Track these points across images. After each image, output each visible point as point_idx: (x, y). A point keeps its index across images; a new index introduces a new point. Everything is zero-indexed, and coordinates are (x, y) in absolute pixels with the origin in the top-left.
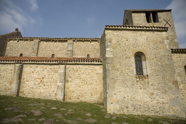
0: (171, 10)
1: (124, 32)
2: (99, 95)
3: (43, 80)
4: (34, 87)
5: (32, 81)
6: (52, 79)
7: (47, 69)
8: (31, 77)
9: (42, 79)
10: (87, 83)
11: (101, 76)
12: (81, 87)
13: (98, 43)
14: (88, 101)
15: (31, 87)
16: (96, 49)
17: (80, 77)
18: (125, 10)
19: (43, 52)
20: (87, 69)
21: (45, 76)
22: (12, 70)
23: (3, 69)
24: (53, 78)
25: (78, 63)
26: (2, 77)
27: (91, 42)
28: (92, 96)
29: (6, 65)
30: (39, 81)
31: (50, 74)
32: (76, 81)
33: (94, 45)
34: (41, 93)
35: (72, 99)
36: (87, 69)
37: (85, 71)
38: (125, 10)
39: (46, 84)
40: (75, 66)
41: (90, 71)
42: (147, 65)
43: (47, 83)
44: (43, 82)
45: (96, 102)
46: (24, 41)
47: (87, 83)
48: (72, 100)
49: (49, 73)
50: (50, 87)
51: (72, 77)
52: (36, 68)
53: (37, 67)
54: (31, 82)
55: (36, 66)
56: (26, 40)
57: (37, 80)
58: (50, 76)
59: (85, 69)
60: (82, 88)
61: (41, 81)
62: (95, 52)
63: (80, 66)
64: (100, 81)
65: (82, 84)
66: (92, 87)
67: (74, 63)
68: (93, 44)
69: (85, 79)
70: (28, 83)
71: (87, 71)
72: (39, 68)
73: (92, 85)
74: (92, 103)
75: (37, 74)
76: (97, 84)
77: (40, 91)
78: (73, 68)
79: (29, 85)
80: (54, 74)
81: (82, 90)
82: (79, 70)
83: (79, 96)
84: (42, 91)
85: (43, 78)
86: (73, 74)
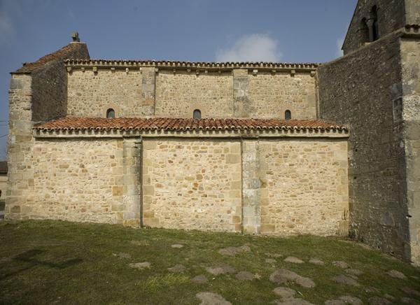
5: (170, 184)
7: (206, 152)
8: (168, 175)
9: (196, 181)
11: (344, 170)
17: (295, 172)
21: (204, 171)
22: (113, 157)
26: (92, 175)
29: (96, 142)
30: (191, 185)
34: (197, 217)
36: (310, 150)
37: (304, 157)
39: (208, 193)
43: (210, 189)
44: (201, 188)
49: (215, 162)
50: (220, 200)
52: (178, 151)
54: (170, 187)
57: (185, 182)
58: (218, 171)
59: (306, 150)
69: (306, 177)
70: (160, 190)
71: (312, 156)
72: (185, 149)
75: (183, 165)
77: (196, 211)
79: (166, 196)
80: (226, 167)
81: (299, 205)
82: (291, 154)
84: (199, 211)
85: (199, 177)
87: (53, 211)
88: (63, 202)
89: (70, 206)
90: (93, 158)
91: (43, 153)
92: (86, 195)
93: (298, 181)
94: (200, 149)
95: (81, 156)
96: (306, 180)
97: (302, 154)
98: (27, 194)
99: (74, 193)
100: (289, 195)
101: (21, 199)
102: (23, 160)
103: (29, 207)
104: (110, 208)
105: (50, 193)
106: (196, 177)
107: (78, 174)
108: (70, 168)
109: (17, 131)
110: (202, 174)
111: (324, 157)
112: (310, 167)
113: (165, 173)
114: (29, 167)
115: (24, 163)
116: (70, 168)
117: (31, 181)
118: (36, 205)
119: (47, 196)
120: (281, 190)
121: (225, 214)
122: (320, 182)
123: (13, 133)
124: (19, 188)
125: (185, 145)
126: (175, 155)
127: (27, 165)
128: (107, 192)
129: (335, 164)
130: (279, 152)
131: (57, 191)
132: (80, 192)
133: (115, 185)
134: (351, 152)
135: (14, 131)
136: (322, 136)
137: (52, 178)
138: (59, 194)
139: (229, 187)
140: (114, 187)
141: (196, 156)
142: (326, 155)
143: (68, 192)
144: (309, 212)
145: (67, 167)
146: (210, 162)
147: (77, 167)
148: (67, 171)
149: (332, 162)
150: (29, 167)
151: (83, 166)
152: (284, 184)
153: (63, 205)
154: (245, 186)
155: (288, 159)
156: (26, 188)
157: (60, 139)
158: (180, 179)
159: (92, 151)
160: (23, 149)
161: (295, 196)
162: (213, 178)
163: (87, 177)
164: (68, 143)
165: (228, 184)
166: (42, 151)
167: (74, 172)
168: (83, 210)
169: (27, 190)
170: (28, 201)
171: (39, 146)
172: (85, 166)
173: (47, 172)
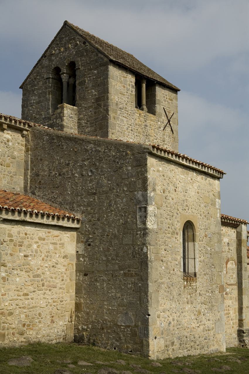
0: (179, 90)
1: (173, 167)
2: (67, 318)
10: (43, 285)
11: (72, 265)
12: (29, 297)
13: (21, 138)
14: (43, 340)
16: (14, 158)
17: (29, 265)
18: (66, 23)
20: (44, 239)
25: (28, 219)
28: (53, 322)
33: (10, 144)
35: (7, 337)
36: (44, 239)
37: (38, 247)
38: (66, 23)
40: (16, 229)
41: (51, 247)
42: (197, 252)
45: (61, 340)
47: (43, 285)
48: (6, 342)
51: (9, 265)
59: (41, 239)
60: (32, 299)
62: (12, 169)
63: (29, 229)
64: (70, 279)
65: (33, 289)
66: (55, 296)
67: (18, 218)
68: (8, 141)
69: (39, 272)
73: (54, 290)
74: (54, 342)
76: (64, 286)
78: (10, 235)
81: (31, 306)
82: (26, 243)
83: (24, 325)
86: (11, 255)
93: (31, 276)
96: (38, 276)
100: (22, 293)
111: (55, 249)
112: (43, 260)
120: (13, 287)
122: (52, 278)
129: (65, 257)
130: (14, 238)
134: (82, 246)
136: (57, 224)
142: (58, 246)
144: (40, 314)
149: (63, 255)
152: (18, 279)
155: (23, 248)
161: (27, 295)
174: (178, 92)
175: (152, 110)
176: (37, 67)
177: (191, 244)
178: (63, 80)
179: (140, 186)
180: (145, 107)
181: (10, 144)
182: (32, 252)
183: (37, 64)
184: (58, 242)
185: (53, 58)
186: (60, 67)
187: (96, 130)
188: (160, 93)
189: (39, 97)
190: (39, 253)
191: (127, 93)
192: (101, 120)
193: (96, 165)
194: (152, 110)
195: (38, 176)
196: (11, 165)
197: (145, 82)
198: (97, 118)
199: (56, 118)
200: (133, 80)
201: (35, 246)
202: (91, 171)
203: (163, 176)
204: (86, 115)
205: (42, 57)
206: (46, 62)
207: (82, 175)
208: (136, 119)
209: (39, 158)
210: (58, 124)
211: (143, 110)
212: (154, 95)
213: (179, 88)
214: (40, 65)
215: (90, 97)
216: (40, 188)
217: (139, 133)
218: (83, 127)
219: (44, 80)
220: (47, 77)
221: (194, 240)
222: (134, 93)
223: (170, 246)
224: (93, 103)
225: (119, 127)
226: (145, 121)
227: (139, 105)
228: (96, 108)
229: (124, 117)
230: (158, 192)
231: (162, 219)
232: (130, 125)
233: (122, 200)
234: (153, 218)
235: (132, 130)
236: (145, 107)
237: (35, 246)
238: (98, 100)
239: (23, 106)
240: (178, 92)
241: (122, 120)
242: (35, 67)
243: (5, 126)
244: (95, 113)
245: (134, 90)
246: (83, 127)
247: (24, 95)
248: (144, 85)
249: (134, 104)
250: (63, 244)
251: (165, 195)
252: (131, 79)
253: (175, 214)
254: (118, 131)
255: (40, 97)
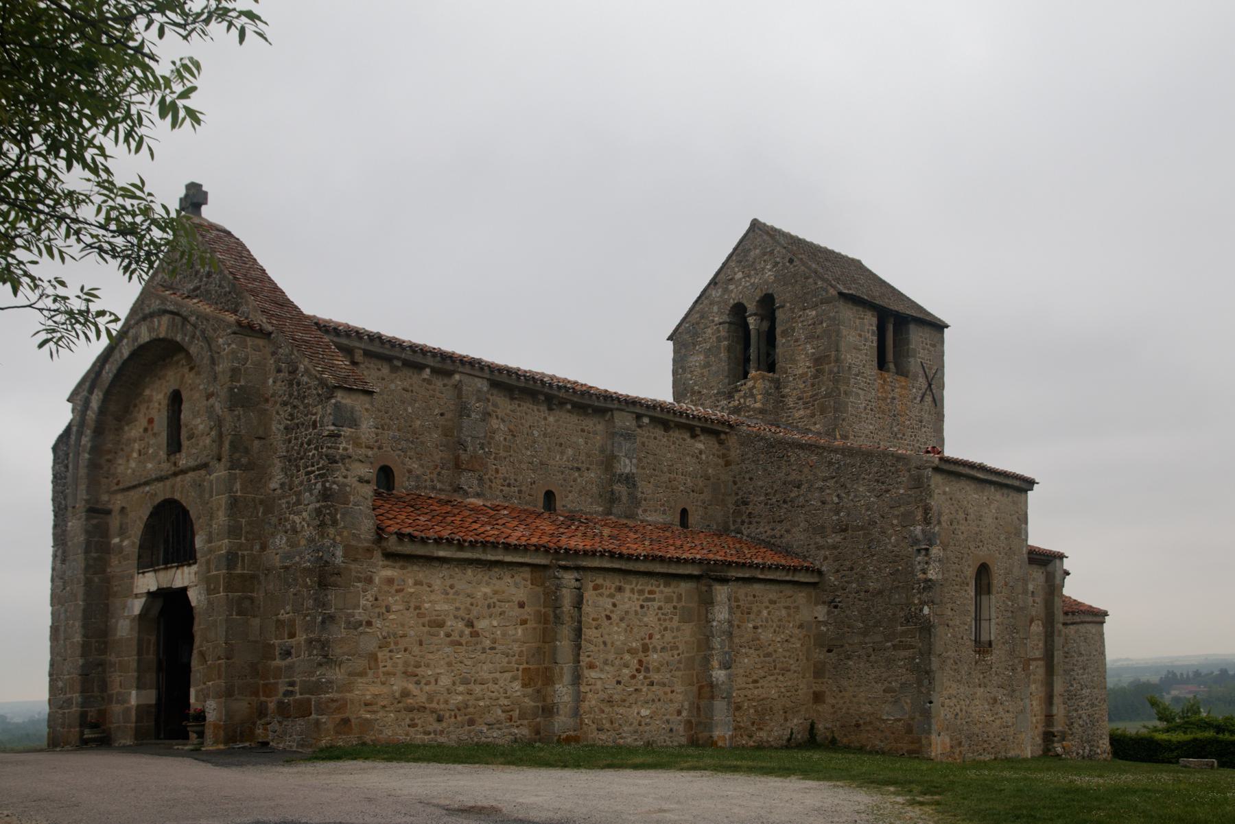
0: (947, 326)
1: (963, 483)
3: (644, 659)
4: (616, 697)
5: (606, 662)
6: (676, 652)
7: (654, 600)
8: (605, 643)
9: (641, 655)
13: (717, 446)
15: (605, 696)
19: (503, 470)
21: (651, 637)
22: (521, 605)
23: (485, 596)
24: (677, 648)
26: (488, 643)
27: (694, 436)
29: (496, 571)
30: (634, 663)
31: (666, 629)
32: (746, 660)
33: (704, 457)
37: (769, 613)
39: (656, 677)
43: (658, 670)
44: (647, 670)
46: (394, 369)
49: (665, 620)
52: (618, 596)
53: (620, 589)
55: (617, 581)
56: (408, 364)
57: (627, 657)
58: (668, 636)
59: (772, 602)
61: (640, 662)
68: (701, 452)
70: (593, 674)
71: (777, 613)
72: (627, 594)
75: (623, 625)
80: (678, 629)
82: (755, 609)
84: (644, 712)
85: (645, 649)
87: (414, 725)
88: (434, 705)
89: (447, 715)
90: (489, 607)
91: (397, 591)
92: (477, 689)
94: (646, 595)
95: (469, 600)
97: (767, 607)
98: (366, 689)
99: (454, 684)
101: (352, 702)
102: (357, 606)
103: (366, 719)
104: (516, 714)
105: (411, 687)
106: (641, 650)
107: (463, 641)
108: (447, 629)
109: (345, 534)
110: (647, 641)
113: (601, 640)
114: (369, 624)
115: (359, 614)
116: (447, 629)
117: (373, 657)
118: (381, 714)
119: (405, 694)
121: (674, 718)
123: (338, 538)
124: (350, 674)
125: (632, 584)
126: (614, 605)
127: (365, 618)
128: (514, 679)
131: (423, 681)
132: (465, 682)
133: (525, 666)
135: (340, 534)
136: (792, 579)
137: (416, 649)
138: (427, 688)
139: (682, 666)
140: (524, 669)
141: (642, 607)
143: (445, 681)
145: (441, 625)
146: (659, 620)
147: (461, 625)
148: (442, 634)
150: (369, 624)
151: (470, 624)
153: (433, 711)
154: (715, 663)
155: (752, 616)
156: (363, 674)
157: (430, 560)
158: (619, 653)
159: (487, 590)
160: (359, 580)
162: (663, 649)
163: (479, 647)
164: (445, 571)
165: (680, 662)
166: (395, 587)
167: (456, 637)
168: (471, 722)
169: (364, 680)
170: (366, 705)
171: (388, 573)
172: (475, 623)
173: (404, 636)
174: (945, 329)
175: (902, 372)
176: (700, 302)
177: (984, 597)
178: (751, 327)
179: (919, 517)
180: (892, 366)
181: (704, 457)
182: (762, 621)
183: (699, 298)
184: (792, 606)
185: (731, 287)
186: (746, 304)
187: (815, 415)
188: (917, 337)
189: (707, 357)
190: (770, 622)
191: (865, 345)
192: (825, 397)
193: (846, 487)
194: (902, 372)
195: (746, 503)
196: (705, 490)
197: (892, 320)
198: (817, 394)
199: (745, 397)
200: (874, 321)
201: (765, 613)
202: (838, 496)
203: (951, 499)
204: (795, 389)
205: (709, 285)
206: (716, 294)
207: (823, 503)
208: (878, 390)
209: (747, 476)
210: (748, 406)
211: (888, 371)
212: (908, 342)
213: (947, 321)
214: (706, 298)
215: (803, 356)
216: (750, 523)
217: (883, 412)
218: (790, 409)
219: (716, 325)
220: (721, 321)
221: (989, 592)
222: (875, 344)
223: (959, 603)
224: (809, 367)
225: (853, 407)
226: (893, 390)
227: (882, 364)
228: (815, 377)
229: (860, 388)
230: (944, 524)
231: (949, 565)
232: (870, 401)
233: (890, 539)
234: (937, 564)
235: (872, 410)
236: (892, 366)
237: (765, 613)
238: (818, 361)
239: (675, 373)
240: (945, 329)
241: (858, 394)
242: (696, 302)
243: (698, 431)
244: (813, 385)
245: (875, 338)
246: (790, 409)
247: (676, 352)
248: (890, 328)
249: (875, 363)
250: (797, 608)
251: (953, 527)
252: (870, 321)
253: (966, 556)
254: (852, 415)
255: (709, 357)
